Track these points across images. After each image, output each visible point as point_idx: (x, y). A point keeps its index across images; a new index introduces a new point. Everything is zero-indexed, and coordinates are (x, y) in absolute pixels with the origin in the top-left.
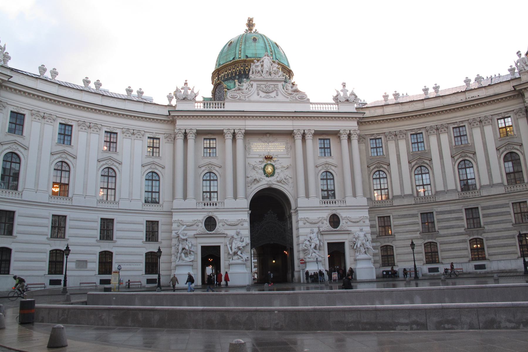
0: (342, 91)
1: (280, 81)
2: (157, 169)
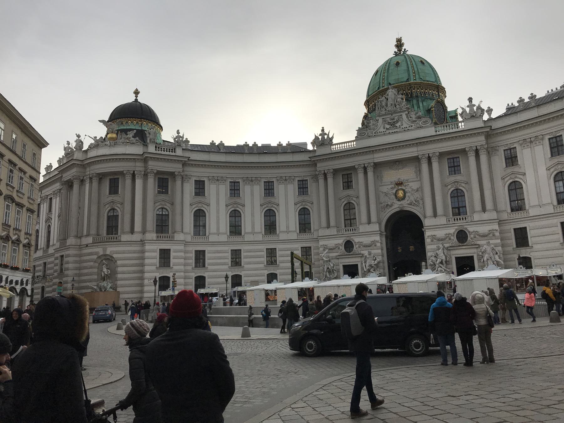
0: (468, 106)
1: (405, 111)
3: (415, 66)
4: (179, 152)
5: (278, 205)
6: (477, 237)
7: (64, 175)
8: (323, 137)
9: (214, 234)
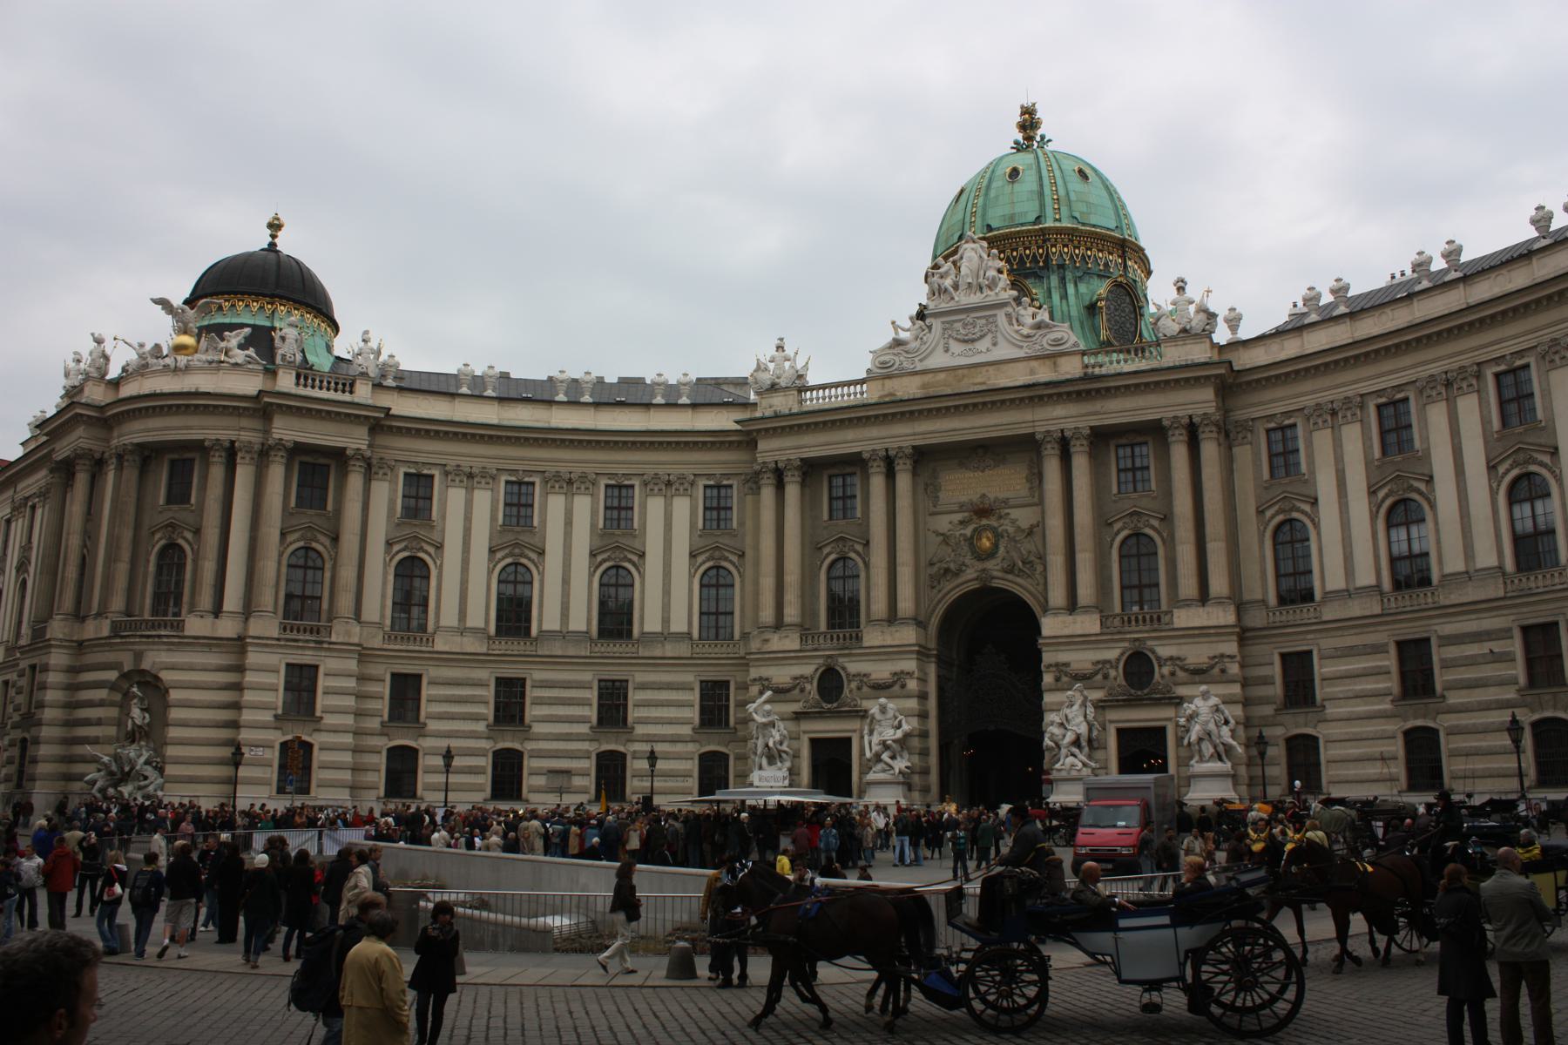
2: (726, 559)
3: (1060, 182)
4: (363, 393)
5: (642, 555)
6: (1180, 674)
7: (57, 446)
9: (450, 630)
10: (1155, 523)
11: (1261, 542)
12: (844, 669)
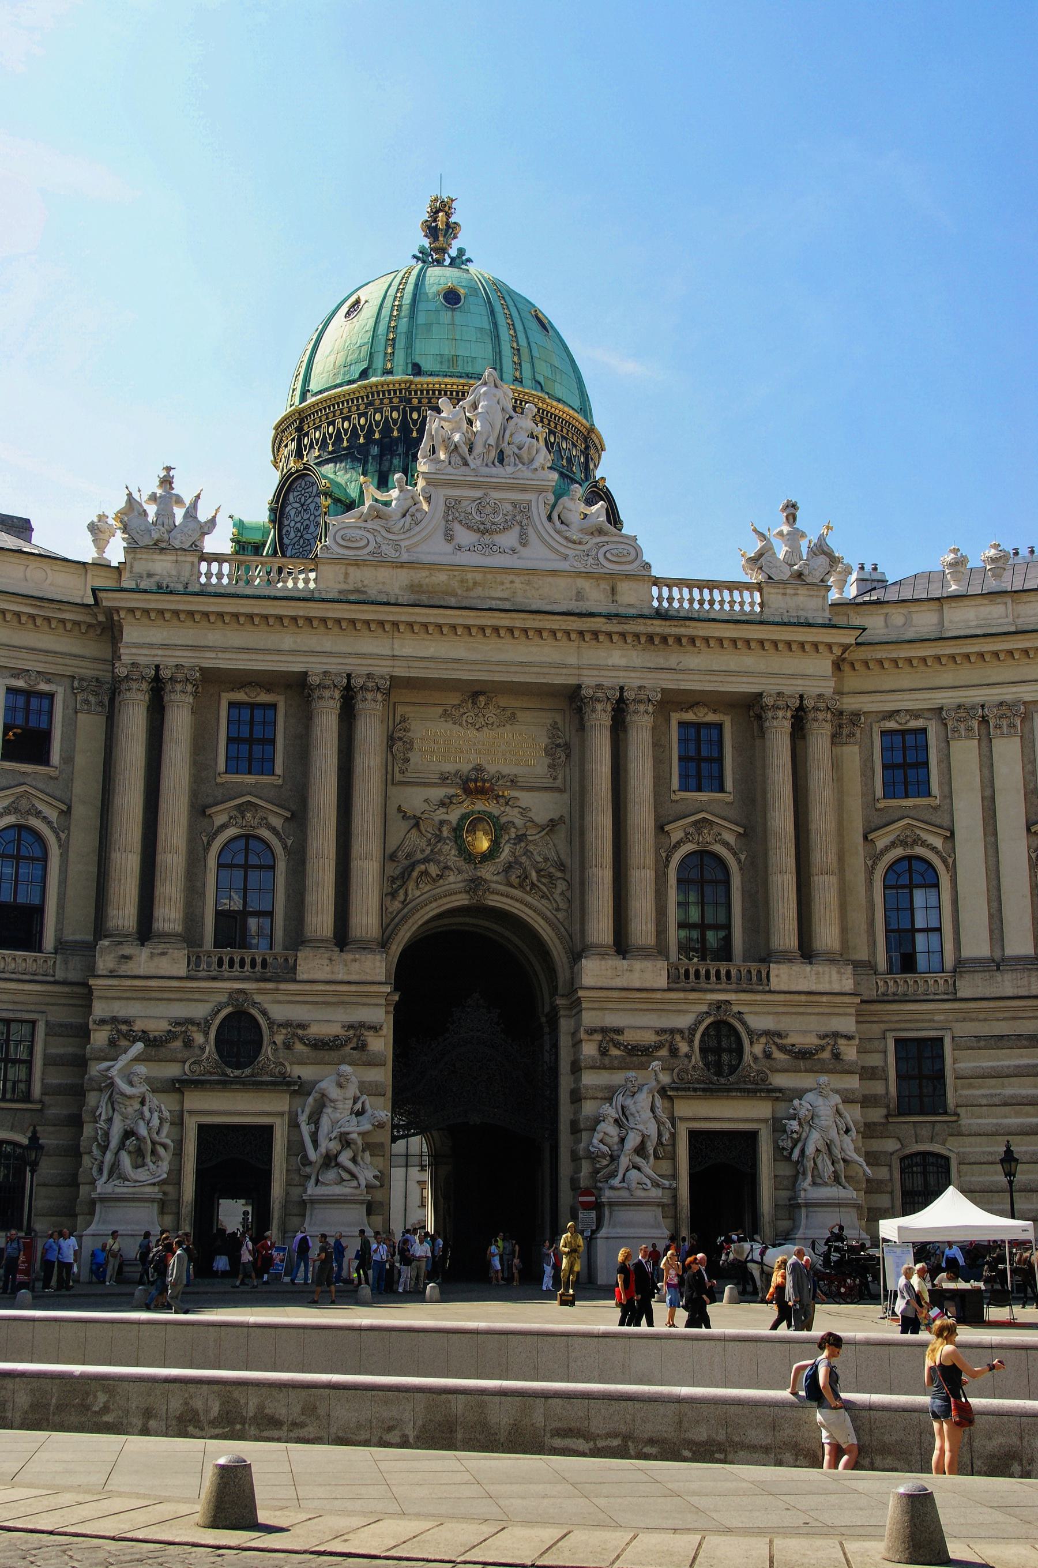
6: (777, 1055)
8: (165, 513)
10: (730, 838)
11: (870, 883)
12: (264, 1013)
